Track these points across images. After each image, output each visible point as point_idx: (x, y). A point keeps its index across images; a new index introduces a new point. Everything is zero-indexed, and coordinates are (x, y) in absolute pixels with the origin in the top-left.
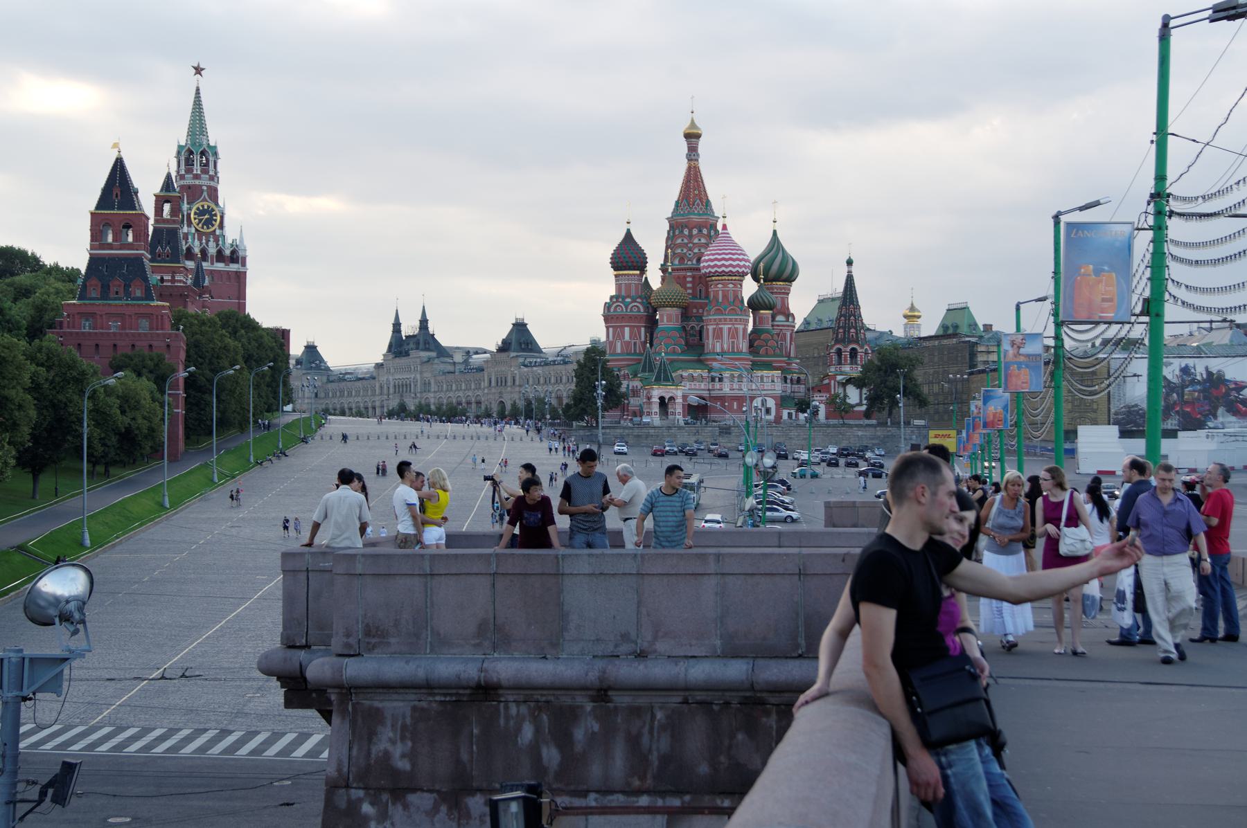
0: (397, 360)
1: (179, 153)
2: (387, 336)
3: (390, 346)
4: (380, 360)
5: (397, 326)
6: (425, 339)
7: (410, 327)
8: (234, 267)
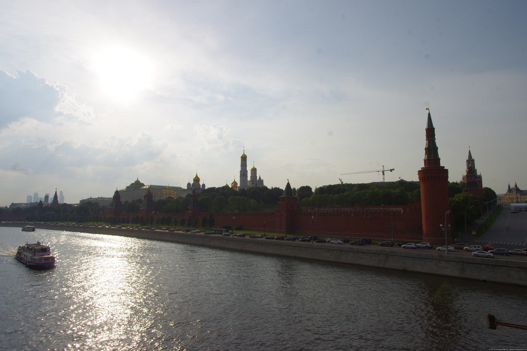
0: (510, 193)
1: (467, 161)
2: (507, 188)
3: (508, 190)
4: (506, 193)
5: (509, 187)
6: (517, 189)
7: (512, 186)
8: (479, 179)
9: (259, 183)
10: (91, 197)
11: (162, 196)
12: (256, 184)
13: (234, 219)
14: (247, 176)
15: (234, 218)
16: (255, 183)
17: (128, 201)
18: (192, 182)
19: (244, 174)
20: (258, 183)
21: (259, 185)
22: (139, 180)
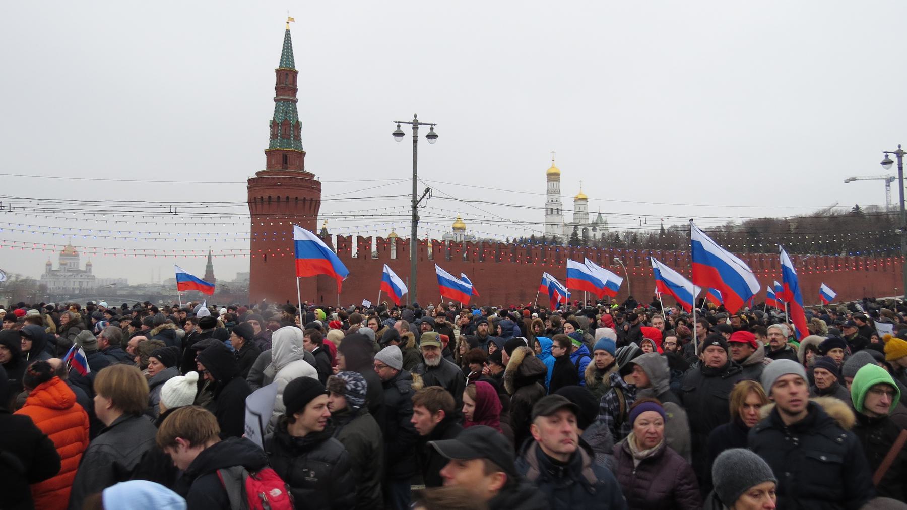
20: (590, 228)
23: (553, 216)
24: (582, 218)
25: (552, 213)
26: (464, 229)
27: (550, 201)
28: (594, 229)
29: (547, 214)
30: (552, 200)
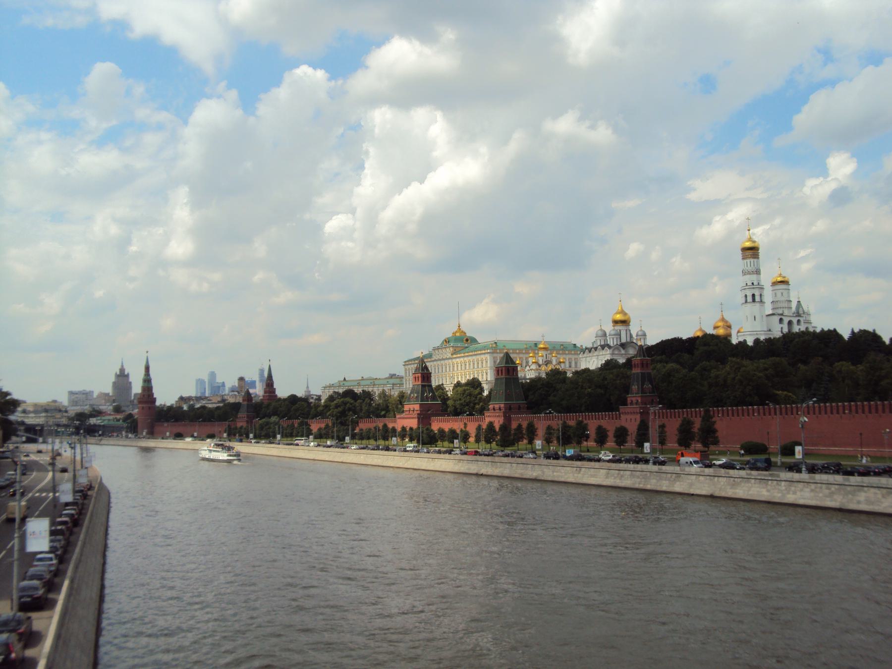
9: (799, 321)
10: (345, 379)
11: (528, 368)
12: (790, 323)
13: (805, 421)
14: (761, 301)
15: (806, 419)
16: (786, 320)
17: (443, 384)
18: (609, 328)
19: (753, 295)
20: (795, 320)
21: (799, 327)
22: (463, 328)
23: (755, 304)
24: (786, 308)
25: (754, 300)
26: (630, 321)
27: (749, 283)
28: (799, 321)
29: (746, 302)
30: (753, 284)
